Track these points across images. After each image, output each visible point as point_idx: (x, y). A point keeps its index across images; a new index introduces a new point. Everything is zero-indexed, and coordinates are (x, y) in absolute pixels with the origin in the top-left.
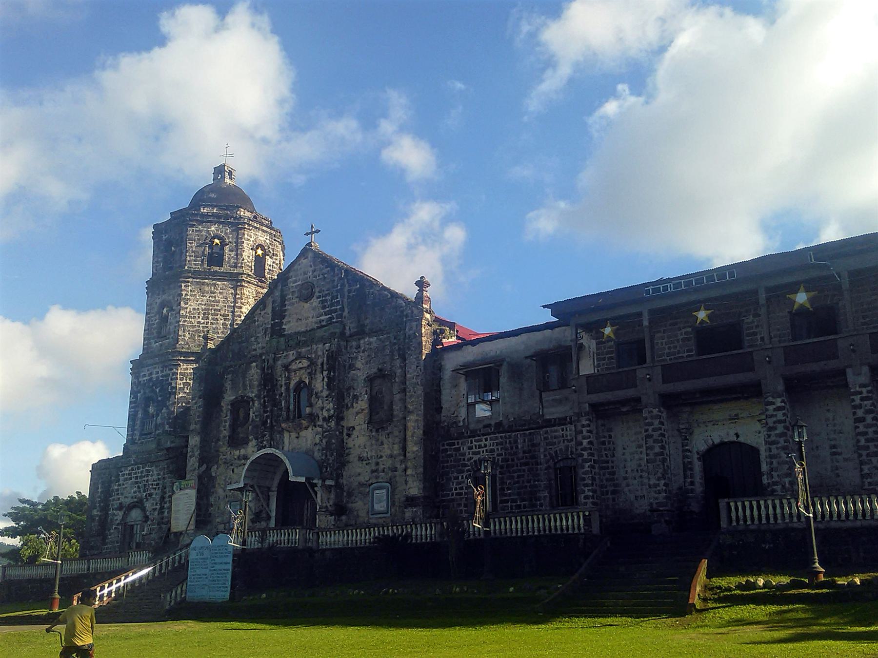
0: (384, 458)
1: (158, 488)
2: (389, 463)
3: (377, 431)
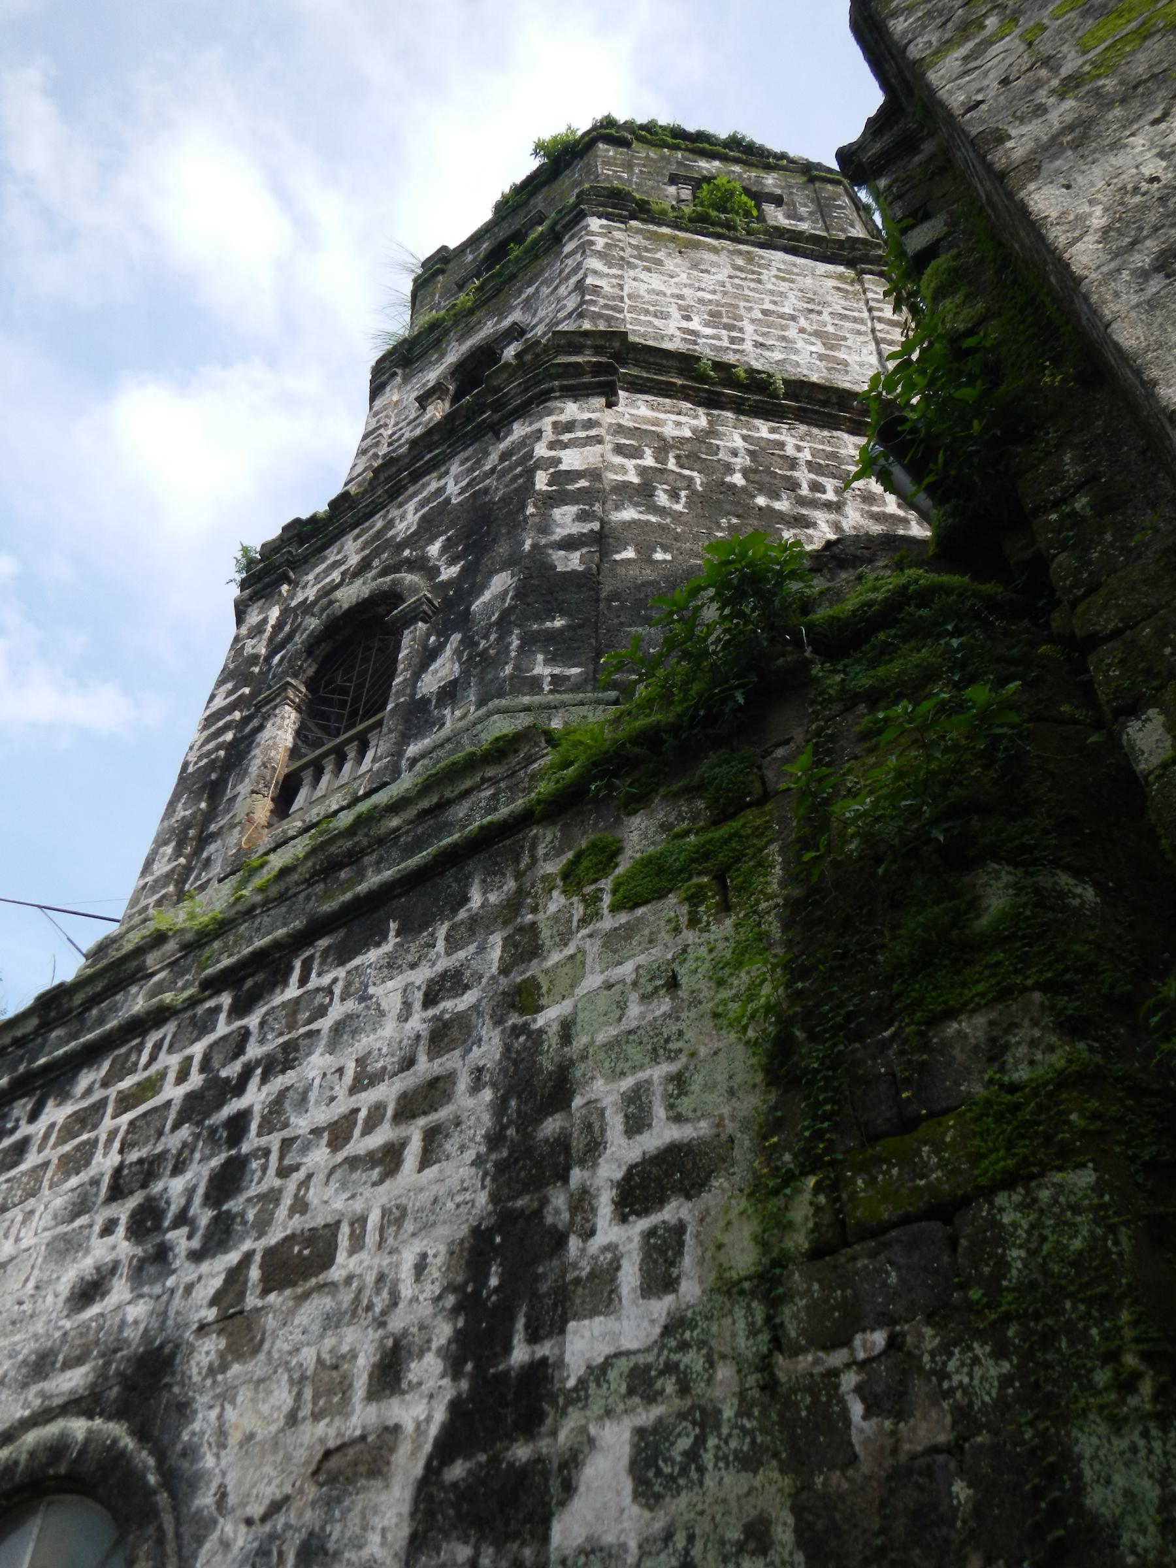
1: (432, 1135)
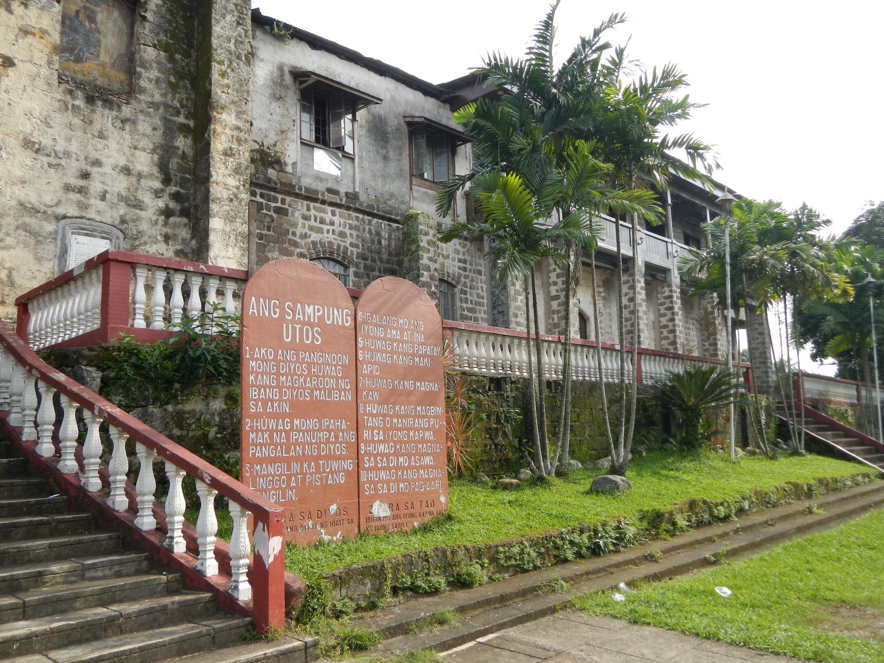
0: (107, 169)
2: (120, 185)
3: (90, 100)
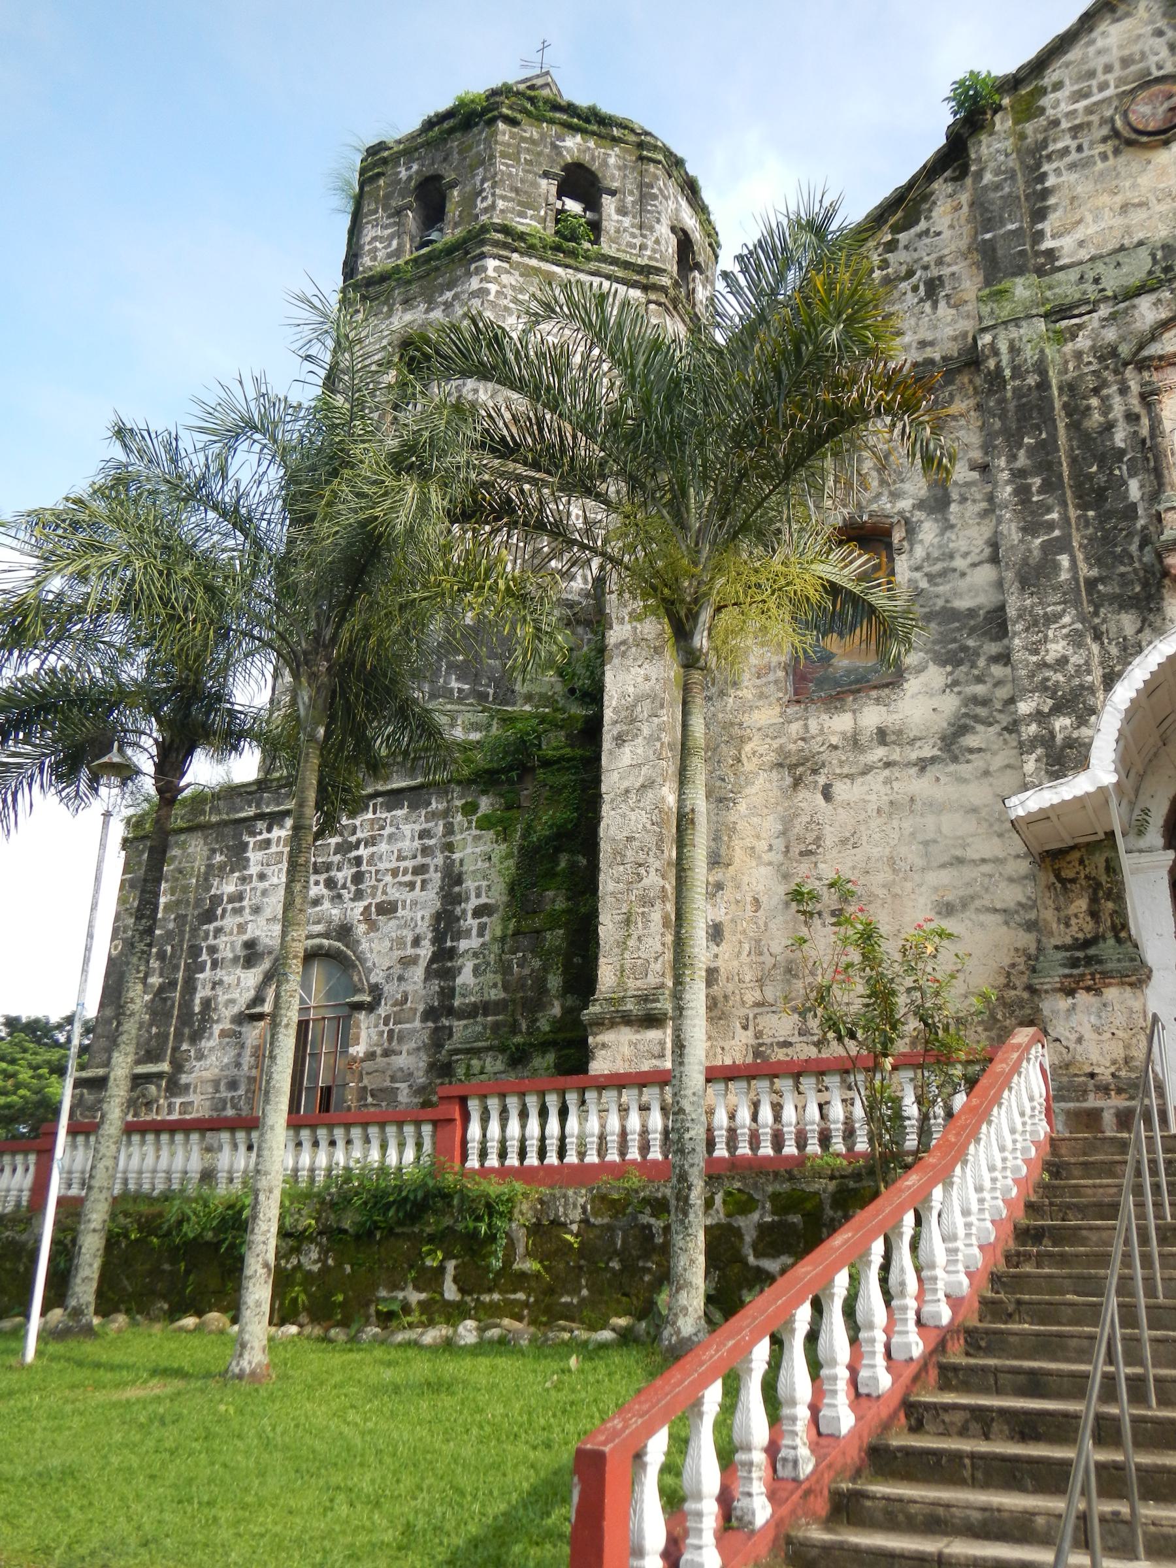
1: (424, 882)
